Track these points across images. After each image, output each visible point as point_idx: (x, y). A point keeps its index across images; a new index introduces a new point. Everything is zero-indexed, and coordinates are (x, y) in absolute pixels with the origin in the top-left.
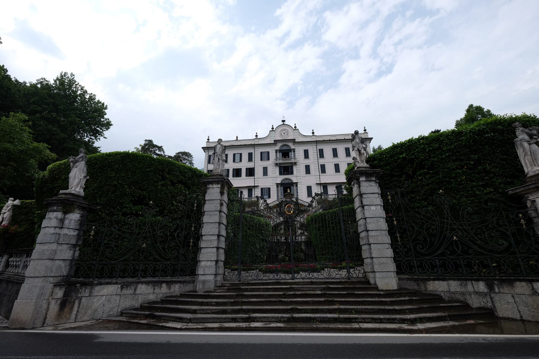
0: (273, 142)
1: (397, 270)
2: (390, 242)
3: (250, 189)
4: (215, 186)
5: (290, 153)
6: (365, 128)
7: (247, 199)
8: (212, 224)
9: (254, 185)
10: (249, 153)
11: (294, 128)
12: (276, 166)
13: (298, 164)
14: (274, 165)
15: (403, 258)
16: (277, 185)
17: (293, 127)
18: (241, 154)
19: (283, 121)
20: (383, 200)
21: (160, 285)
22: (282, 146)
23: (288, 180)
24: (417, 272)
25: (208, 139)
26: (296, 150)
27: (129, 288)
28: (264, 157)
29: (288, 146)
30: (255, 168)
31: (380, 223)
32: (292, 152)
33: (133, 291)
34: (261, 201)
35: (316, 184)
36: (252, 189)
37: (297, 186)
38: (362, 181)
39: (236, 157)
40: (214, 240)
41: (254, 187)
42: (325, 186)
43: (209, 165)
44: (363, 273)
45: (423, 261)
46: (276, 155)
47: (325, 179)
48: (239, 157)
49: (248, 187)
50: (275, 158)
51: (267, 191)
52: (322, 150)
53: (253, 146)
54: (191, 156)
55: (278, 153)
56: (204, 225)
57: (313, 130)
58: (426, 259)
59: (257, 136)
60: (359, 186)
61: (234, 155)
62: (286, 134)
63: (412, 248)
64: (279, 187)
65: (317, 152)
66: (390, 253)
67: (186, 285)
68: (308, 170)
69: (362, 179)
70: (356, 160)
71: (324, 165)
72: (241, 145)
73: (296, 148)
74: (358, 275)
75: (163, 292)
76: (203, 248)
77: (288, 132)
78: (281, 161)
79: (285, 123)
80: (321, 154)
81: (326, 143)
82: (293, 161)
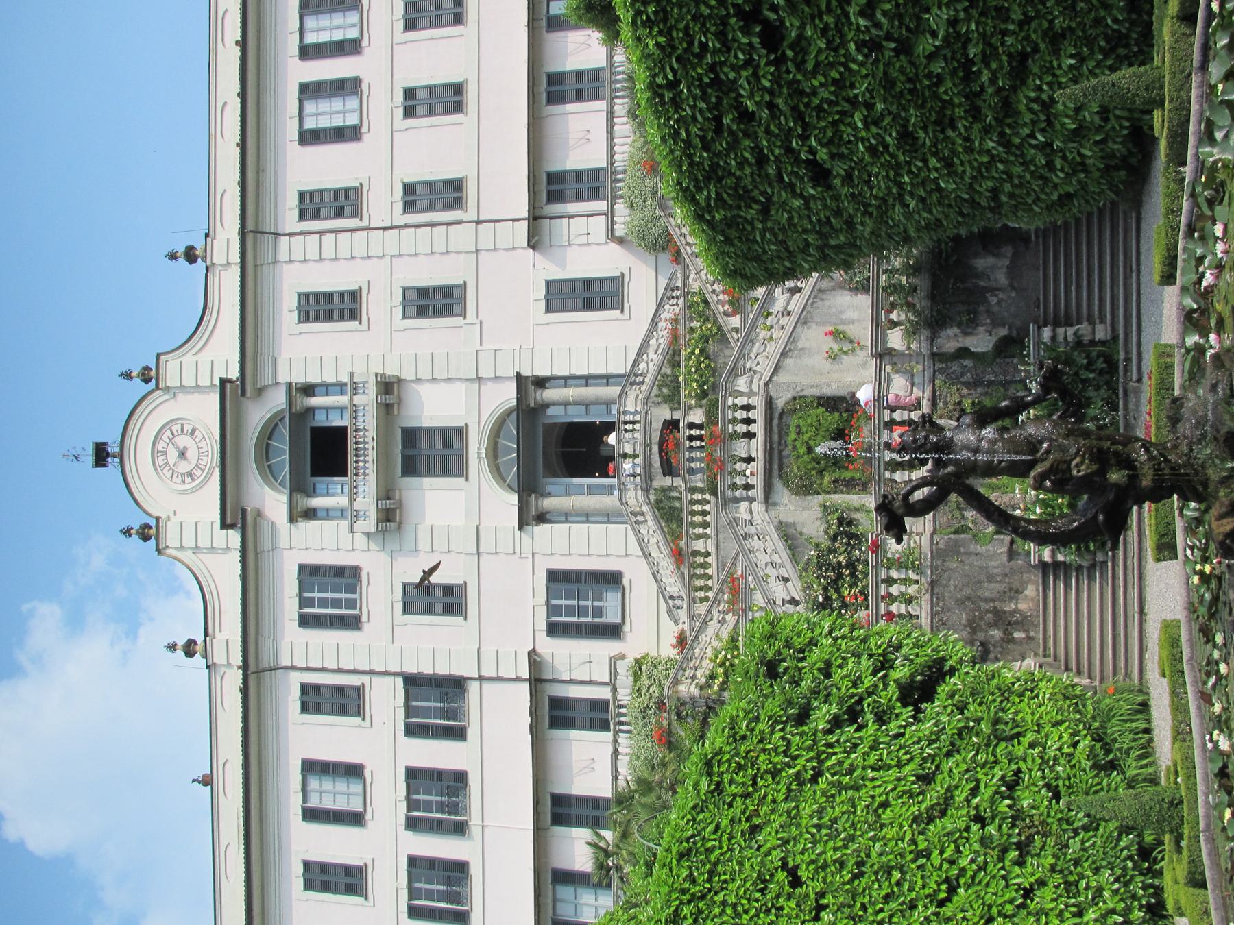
0: (234, 537)
5: (321, 420)
9: (527, 685)
10: (306, 708)
11: (152, 384)
13: (391, 370)
16: (529, 517)
17: (140, 388)
18: (311, 767)
19: (101, 455)
22: (268, 471)
23: (502, 442)
26: (299, 379)
28: (337, 603)
29: (269, 431)
30: (411, 669)
37: (541, 383)
39: (327, 803)
46: (328, 514)
48: (327, 784)
49: (535, 729)
50: (345, 524)
57: (173, 256)
59: (189, 649)
61: (311, 815)
62: (183, 441)
65: (322, 233)
71: (409, 188)
73: (283, 378)
78: (368, 486)
79: (113, 449)
81: (259, 170)
82: (368, 399)
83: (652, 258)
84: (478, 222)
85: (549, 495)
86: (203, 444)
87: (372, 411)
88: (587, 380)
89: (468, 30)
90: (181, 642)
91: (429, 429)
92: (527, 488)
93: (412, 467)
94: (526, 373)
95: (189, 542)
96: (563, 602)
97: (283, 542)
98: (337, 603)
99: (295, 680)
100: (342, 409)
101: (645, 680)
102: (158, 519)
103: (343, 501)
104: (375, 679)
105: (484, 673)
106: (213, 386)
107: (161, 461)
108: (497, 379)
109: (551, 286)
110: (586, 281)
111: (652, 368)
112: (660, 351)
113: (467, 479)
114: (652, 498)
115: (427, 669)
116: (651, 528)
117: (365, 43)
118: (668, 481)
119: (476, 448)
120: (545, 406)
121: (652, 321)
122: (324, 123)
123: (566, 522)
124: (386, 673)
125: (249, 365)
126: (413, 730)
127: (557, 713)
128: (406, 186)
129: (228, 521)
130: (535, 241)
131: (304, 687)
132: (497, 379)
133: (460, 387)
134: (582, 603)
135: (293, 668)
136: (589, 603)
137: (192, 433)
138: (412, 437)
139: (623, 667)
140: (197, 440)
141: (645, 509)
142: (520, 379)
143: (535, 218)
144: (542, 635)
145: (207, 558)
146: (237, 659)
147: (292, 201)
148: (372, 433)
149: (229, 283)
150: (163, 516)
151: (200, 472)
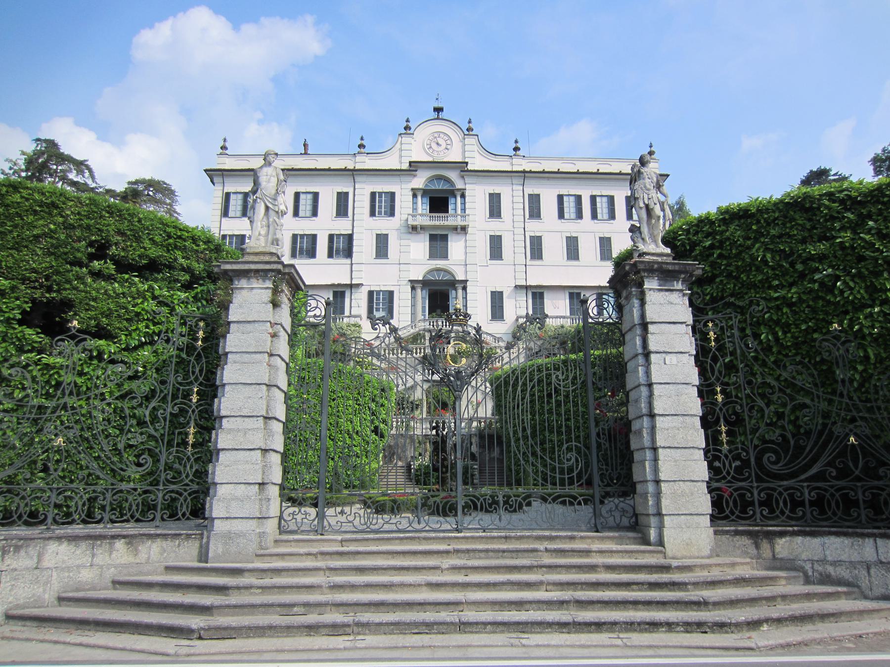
0: (405, 166)
1: (712, 510)
2: (704, 446)
3: (339, 293)
4: (255, 283)
5: (451, 201)
6: (651, 146)
8: (247, 388)
9: (349, 282)
11: (466, 133)
13: (470, 230)
15: (729, 482)
16: (414, 284)
18: (316, 195)
19: (438, 110)
20: (696, 340)
21: (110, 543)
22: (431, 180)
24: (758, 515)
25: (224, 148)
26: (467, 194)
27: (23, 552)
28: (380, 207)
29: (447, 180)
30: (355, 237)
31: (684, 396)
32: (459, 199)
33: (36, 560)
34: (382, 328)
36: (343, 294)
37: (464, 288)
38: (650, 289)
39: (302, 202)
40: (253, 429)
41: (351, 286)
42: (538, 294)
43: (224, 220)
44: (632, 517)
45: (774, 490)
46: (415, 203)
47: (538, 276)
49: (333, 285)
53: (352, 173)
54: (173, 192)
55: (419, 198)
56: (227, 388)
57: (516, 142)
58: (780, 486)
60: (643, 303)
63: (753, 460)
64: (419, 291)
66: (702, 470)
67: (179, 545)
68: (496, 247)
69: (650, 284)
70: (638, 234)
72: (316, 170)
73: (468, 187)
74: (618, 521)
75: (118, 562)
76: (223, 449)
77: (449, 142)
78: (426, 221)
79: (441, 115)
80: (534, 209)
81: (548, 178)
82: (459, 222)
83: (510, 332)
84: (526, 265)
87: (454, 223)
89: (598, 262)
91: (447, 245)
92: (425, 283)
93: (433, 238)
95: (404, 147)
96: (381, 297)
97: (404, 186)
98: (380, 207)
99: (350, 190)
100: (455, 210)
101: (353, 328)
102: (413, 134)
103: (420, 211)
104: (351, 222)
105: (354, 265)
106: (465, 158)
107: (436, 135)
108: (466, 272)
109: (501, 294)
110: (502, 307)
114: (421, 332)
115: (355, 243)
117: (596, 221)
119: (440, 263)
120: (456, 289)
122: (566, 204)
125: (473, 173)
126: (331, 237)
127: (339, 294)
128: (540, 237)
131: (347, 194)
132: (466, 272)
133: (463, 258)
135: (355, 189)
137: (446, 149)
138: (445, 238)
139: (358, 320)
141: (417, 329)
142: (466, 281)
143: (527, 288)
144: (368, 289)
145: (397, 155)
147: (536, 192)
148: (446, 223)
149: (504, 165)
150: (414, 136)
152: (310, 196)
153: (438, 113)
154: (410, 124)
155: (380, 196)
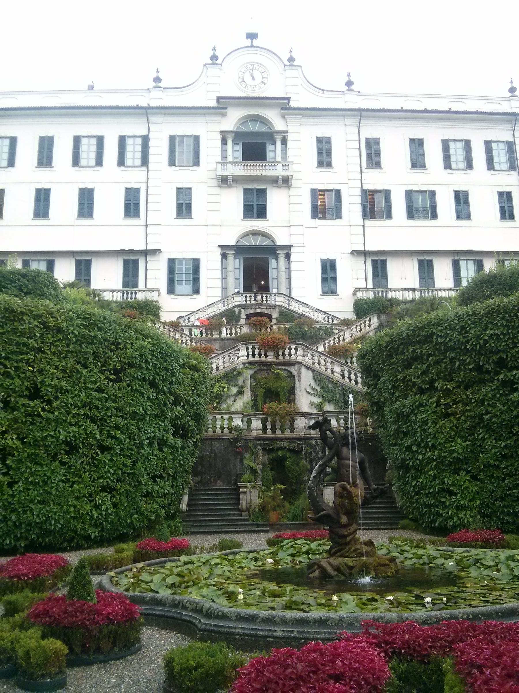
0: (213, 103)
5: (270, 148)
7: (120, 294)
11: (287, 63)
12: (219, 186)
13: (294, 183)
14: (215, 183)
19: (252, 36)
26: (290, 137)
32: (278, 143)
35: (353, 253)
36: (136, 262)
37: (288, 257)
39: (84, 148)
41: (146, 253)
46: (224, 152)
49: (122, 252)
50: (219, 159)
51: (187, 269)
52: (377, 141)
55: (230, 143)
57: (349, 75)
59: (157, 80)
61: (77, 140)
62: (258, 77)
73: (290, 129)
77: (265, 75)
78: (240, 171)
79: (255, 42)
81: (390, 118)
82: (279, 171)
84: (364, 226)
85: (235, 259)
86: (258, 88)
88: (289, 278)
90: (160, 76)
94: (293, 250)
96: (184, 267)
102: (221, 64)
103: (230, 158)
105: (149, 227)
111: (296, 309)
112: (304, 313)
113: (242, 220)
116: (221, 308)
118: (243, 316)
121: (318, 309)
123: (222, 268)
124: (148, 178)
129: (221, 100)
130: (355, 253)
134: (184, 275)
136: (184, 279)
137: (263, 82)
140: (260, 85)
143: (365, 254)
146: (153, 104)
148: (264, 173)
151: (244, 86)
152: (94, 141)
153: (252, 40)
154: (217, 54)
155: (181, 142)
